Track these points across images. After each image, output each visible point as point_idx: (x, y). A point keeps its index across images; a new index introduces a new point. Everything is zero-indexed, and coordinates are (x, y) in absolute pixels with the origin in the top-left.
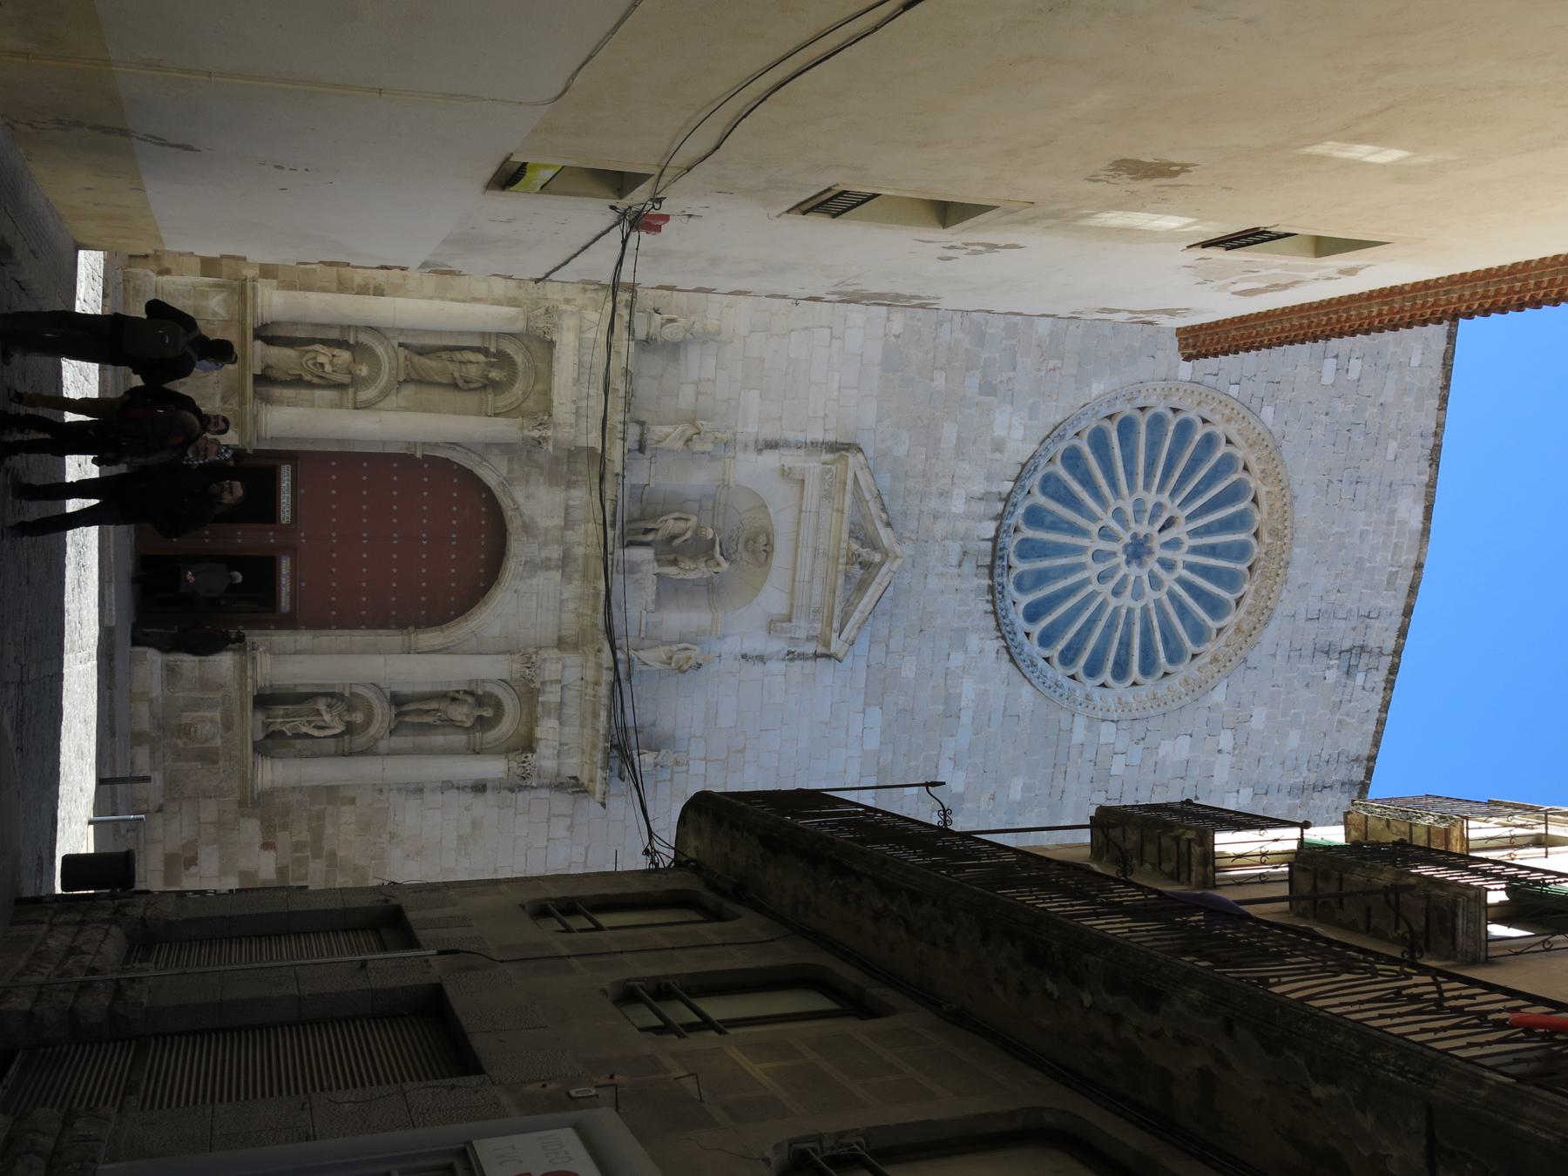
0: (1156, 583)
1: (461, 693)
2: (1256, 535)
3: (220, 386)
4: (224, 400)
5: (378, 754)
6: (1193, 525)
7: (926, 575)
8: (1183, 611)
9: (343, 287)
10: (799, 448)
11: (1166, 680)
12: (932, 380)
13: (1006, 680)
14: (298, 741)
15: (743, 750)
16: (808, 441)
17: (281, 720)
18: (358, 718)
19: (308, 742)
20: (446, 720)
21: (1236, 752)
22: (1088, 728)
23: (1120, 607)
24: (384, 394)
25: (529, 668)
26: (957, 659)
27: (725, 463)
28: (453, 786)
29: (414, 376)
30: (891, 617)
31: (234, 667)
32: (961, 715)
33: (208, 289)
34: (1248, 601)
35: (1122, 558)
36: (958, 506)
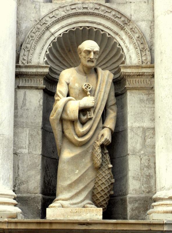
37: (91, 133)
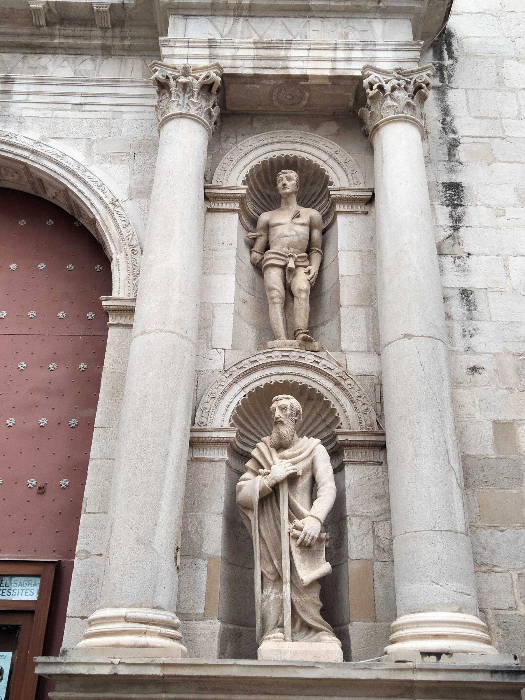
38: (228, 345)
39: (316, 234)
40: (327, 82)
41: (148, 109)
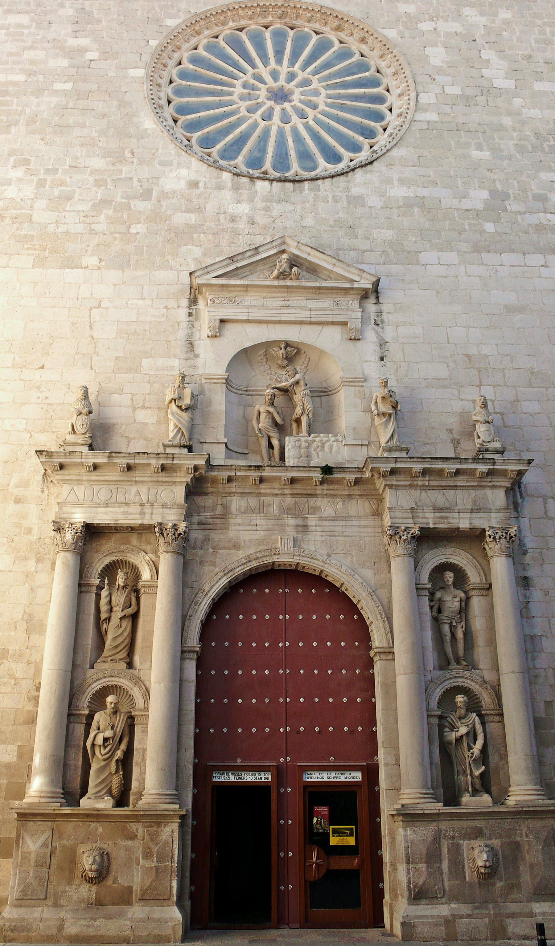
0: (306, 83)
1: (432, 604)
2: (267, 27)
3: (119, 841)
4: (133, 837)
5: (499, 680)
6: (258, 61)
7: (302, 226)
8: (327, 65)
9: (32, 721)
10: (193, 326)
11: (383, 71)
12: (138, 233)
13: (390, 167)
14: (491, 760)
15: (468, 356)
16: (188, 320)
17: (469, 777)
18: (462, 699)
19: (491, 750)
20: (460, 617)
21: (435, 19)
22: (425, 111)
23: (325, 102)
24: (138, 681)
25: (400, 537)
26: (374, 201)
27: (206, 383)
28: (526, 607)
29: (123, 655)
30: (340, 250)
31: (414, 826)
32: (421, 195)
33: (20, 853)
34: (317, 26)
35: (286, 105)
36: (244, 209)
37: (110, 753)
38: (432, 668)
39: (463, 604)
40: (468, 530)
41: (377, 534)
